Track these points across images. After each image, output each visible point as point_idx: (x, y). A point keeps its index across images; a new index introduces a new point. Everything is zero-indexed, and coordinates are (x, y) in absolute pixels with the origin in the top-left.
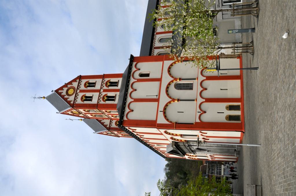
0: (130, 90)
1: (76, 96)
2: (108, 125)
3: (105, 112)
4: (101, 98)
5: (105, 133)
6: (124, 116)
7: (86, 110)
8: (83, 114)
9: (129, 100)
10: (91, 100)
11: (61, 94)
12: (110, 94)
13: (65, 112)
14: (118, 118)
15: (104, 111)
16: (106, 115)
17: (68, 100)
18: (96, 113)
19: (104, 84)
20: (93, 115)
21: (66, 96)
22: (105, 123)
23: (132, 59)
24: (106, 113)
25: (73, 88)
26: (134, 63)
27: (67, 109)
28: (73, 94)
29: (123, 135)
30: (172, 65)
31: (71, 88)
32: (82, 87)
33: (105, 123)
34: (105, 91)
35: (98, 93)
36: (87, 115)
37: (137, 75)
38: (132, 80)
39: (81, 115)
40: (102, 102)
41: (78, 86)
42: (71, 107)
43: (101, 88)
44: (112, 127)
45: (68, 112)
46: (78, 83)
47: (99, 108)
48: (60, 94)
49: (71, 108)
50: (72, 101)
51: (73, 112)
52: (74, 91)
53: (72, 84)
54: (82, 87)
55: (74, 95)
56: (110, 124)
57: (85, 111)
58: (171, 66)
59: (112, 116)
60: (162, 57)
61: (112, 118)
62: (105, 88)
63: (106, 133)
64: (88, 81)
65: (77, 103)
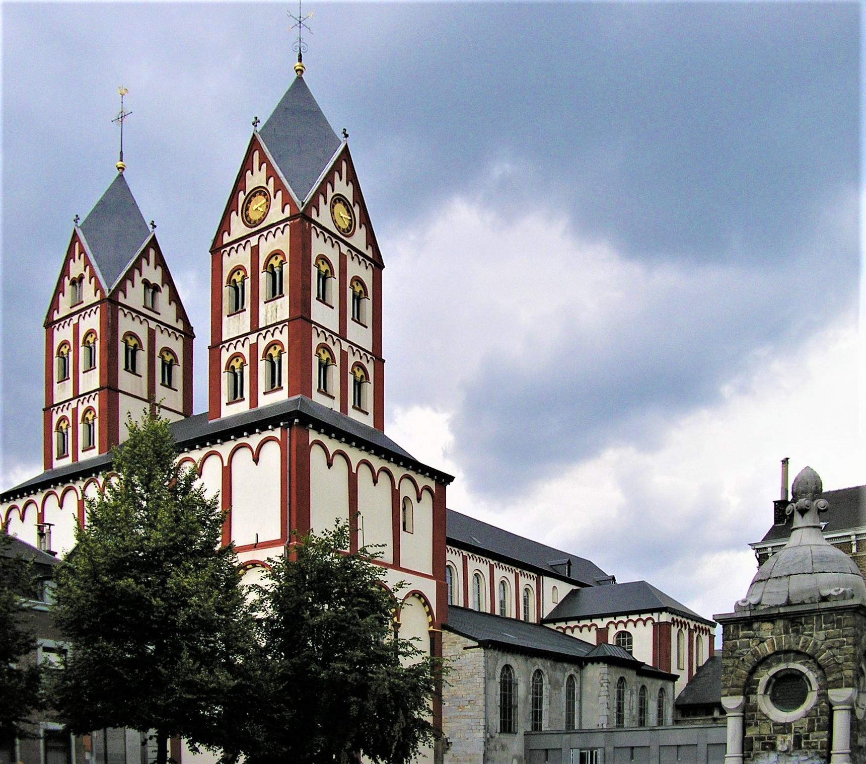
2: (125, 297)
3: (269, 338)
5: (77, 268)
12: (335, 372)
22: (133, 286)
30: (426, 603)
34: (344, 355)
40: (316, 341)
44: (121, 314)
58: (423, 601)
60: (440, 571)
62: (352, 360)
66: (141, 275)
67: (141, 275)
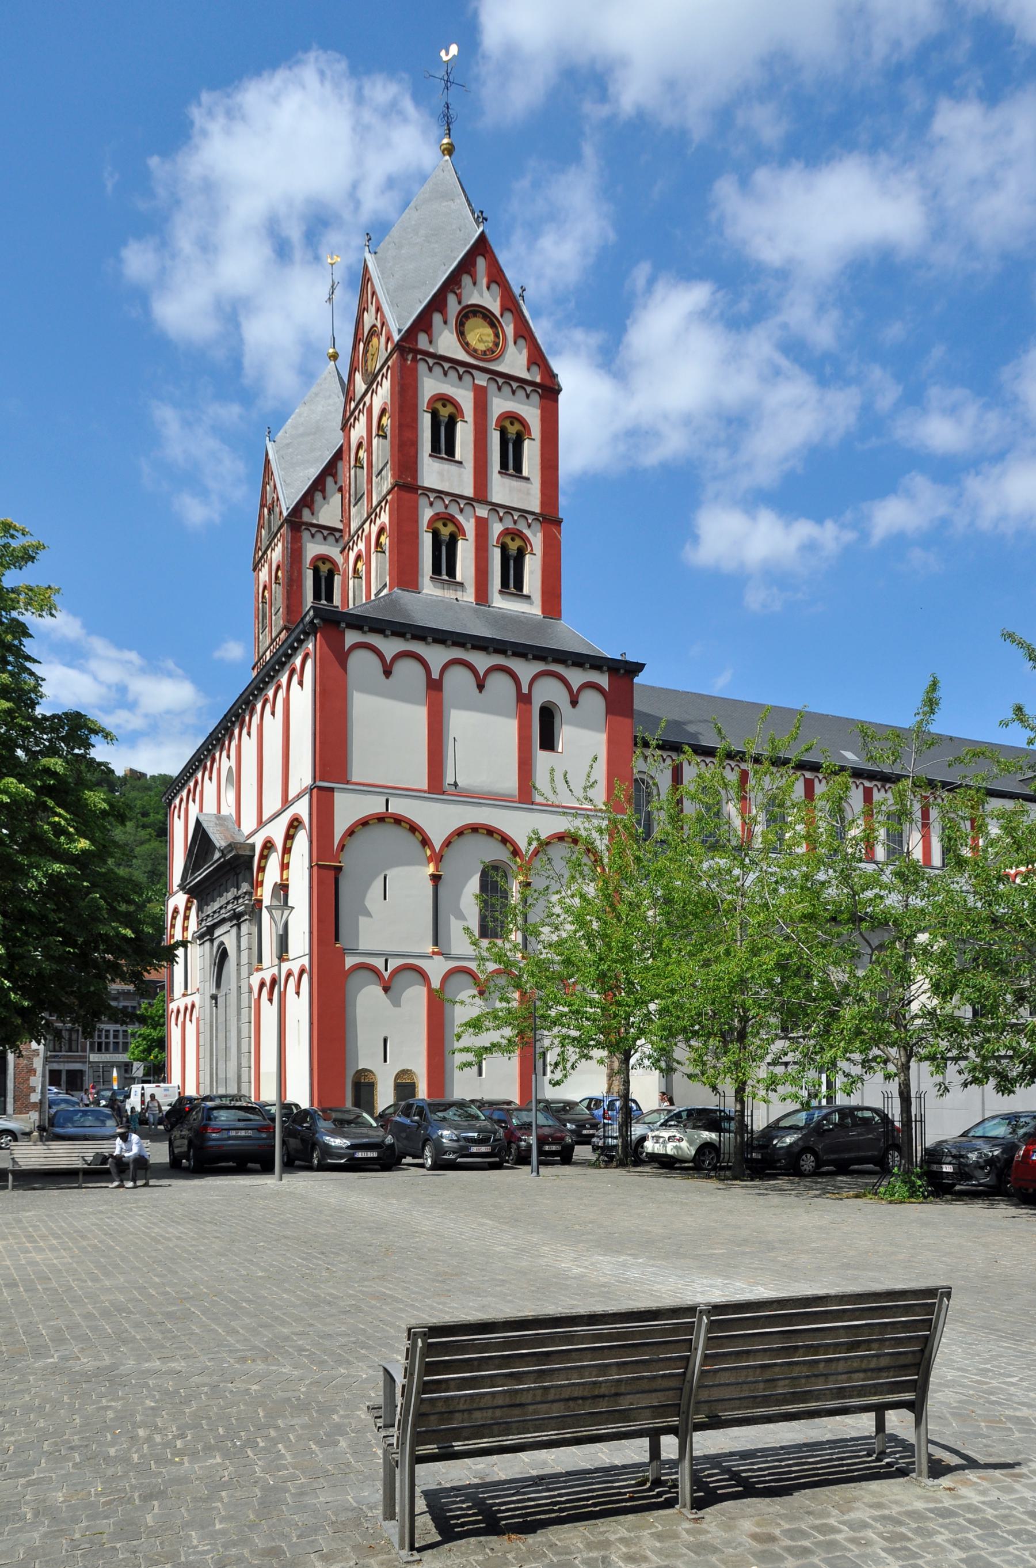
0: (482, 661)
1: (456, 363)
4: (446, 507)
6: (364, 632)
7: (385, 421)
8: (367, 399)
9: (437, 656)
10: (435, 449)
11: (466, 273)
13: (374, 293)
14: (351, 582)
15: (385, 518)
16: (366, 526)
17: (437, 318)
18: (375, 471)
19: (515, 522)
20: (362, 454)
21: (459, 308)
22: (324, 498)
23: (622, 671)
24: (375, 529)
25: (496, 345)
26: (603, 680)
27: (386, 308)
28: (466, 346)
29: (266, 593)
31: (497, 335)
32: (500, 405)
33: (324, 498)
34: (482, 526)
35: (469, 491)
36: (363, 418)
37: (549, 691)
38: (525, 670)
39: (360, 386)
41: (508, 378)
42: (402, 340)
43: (495, 507)
44: (306, 535)
45: (372, 309)
46: (524, 374)
47: (399, 500)
48: (466, 266)
49: (396, 337)
50: (431, 342)
51: (375, 340)
52: (484, 353)
53: (515, 343)
54: (500, 405)
55: (462, 356)
56: (321, 527)
57: (383, 412)
59: (358, 557)
61: (352, 556)
63: (269, 502)
64: (530, 434)
65: (422, 367)
66: (336, 483)
67: (336, 483)
